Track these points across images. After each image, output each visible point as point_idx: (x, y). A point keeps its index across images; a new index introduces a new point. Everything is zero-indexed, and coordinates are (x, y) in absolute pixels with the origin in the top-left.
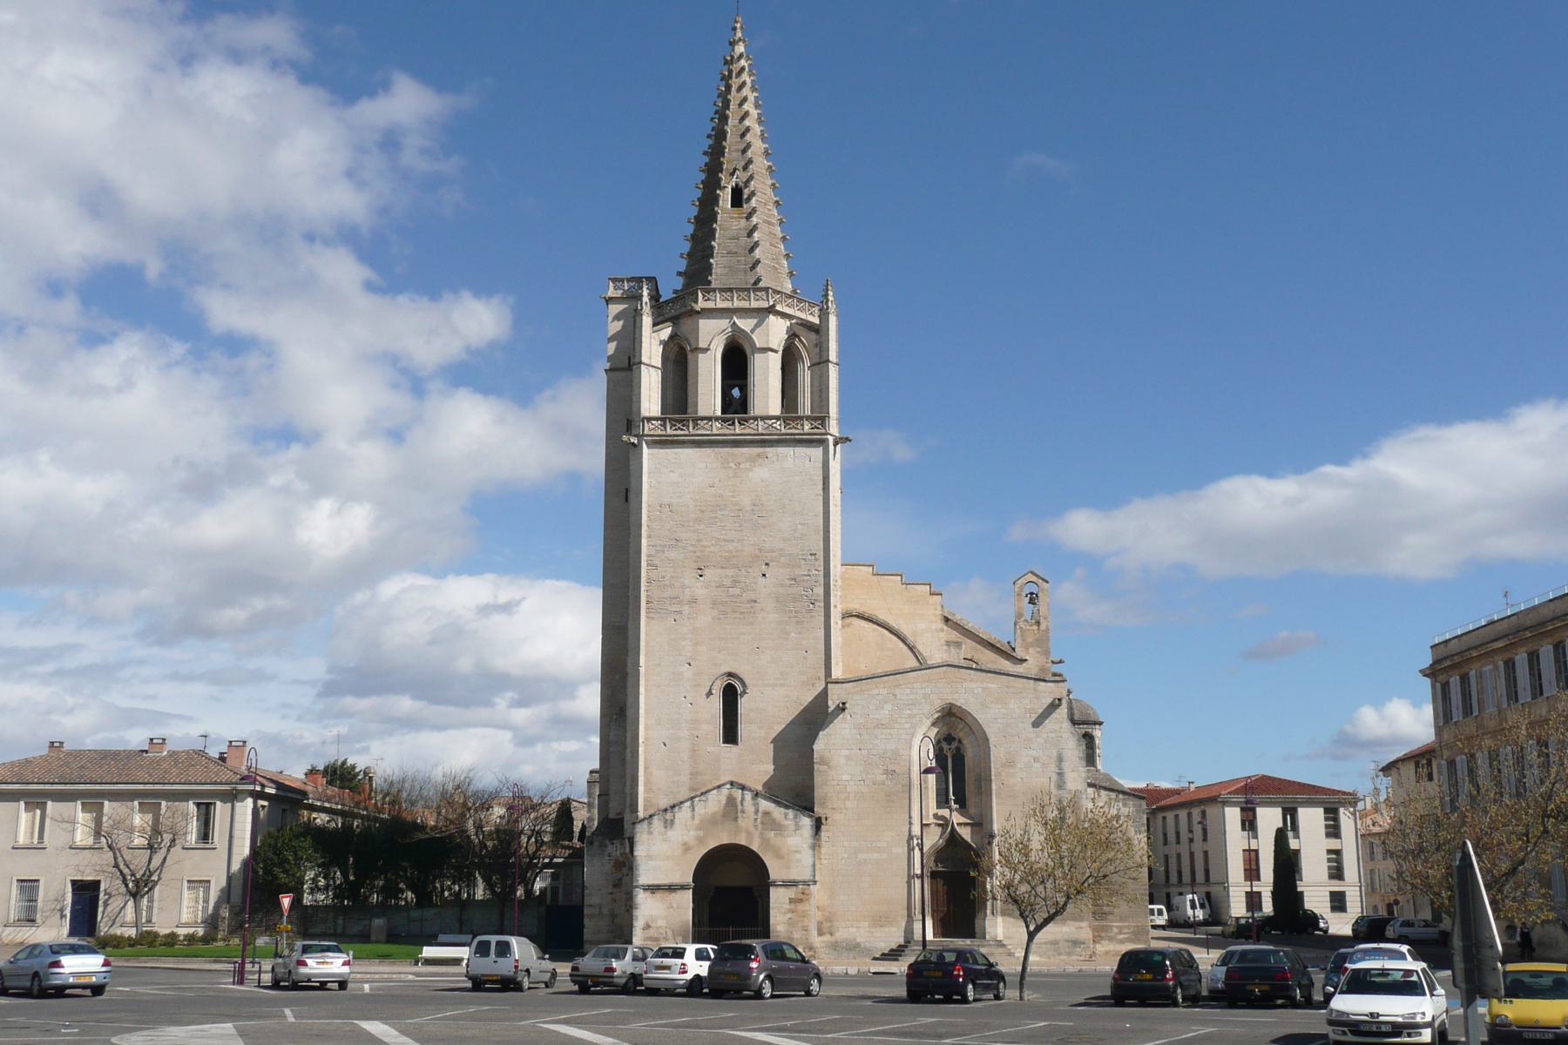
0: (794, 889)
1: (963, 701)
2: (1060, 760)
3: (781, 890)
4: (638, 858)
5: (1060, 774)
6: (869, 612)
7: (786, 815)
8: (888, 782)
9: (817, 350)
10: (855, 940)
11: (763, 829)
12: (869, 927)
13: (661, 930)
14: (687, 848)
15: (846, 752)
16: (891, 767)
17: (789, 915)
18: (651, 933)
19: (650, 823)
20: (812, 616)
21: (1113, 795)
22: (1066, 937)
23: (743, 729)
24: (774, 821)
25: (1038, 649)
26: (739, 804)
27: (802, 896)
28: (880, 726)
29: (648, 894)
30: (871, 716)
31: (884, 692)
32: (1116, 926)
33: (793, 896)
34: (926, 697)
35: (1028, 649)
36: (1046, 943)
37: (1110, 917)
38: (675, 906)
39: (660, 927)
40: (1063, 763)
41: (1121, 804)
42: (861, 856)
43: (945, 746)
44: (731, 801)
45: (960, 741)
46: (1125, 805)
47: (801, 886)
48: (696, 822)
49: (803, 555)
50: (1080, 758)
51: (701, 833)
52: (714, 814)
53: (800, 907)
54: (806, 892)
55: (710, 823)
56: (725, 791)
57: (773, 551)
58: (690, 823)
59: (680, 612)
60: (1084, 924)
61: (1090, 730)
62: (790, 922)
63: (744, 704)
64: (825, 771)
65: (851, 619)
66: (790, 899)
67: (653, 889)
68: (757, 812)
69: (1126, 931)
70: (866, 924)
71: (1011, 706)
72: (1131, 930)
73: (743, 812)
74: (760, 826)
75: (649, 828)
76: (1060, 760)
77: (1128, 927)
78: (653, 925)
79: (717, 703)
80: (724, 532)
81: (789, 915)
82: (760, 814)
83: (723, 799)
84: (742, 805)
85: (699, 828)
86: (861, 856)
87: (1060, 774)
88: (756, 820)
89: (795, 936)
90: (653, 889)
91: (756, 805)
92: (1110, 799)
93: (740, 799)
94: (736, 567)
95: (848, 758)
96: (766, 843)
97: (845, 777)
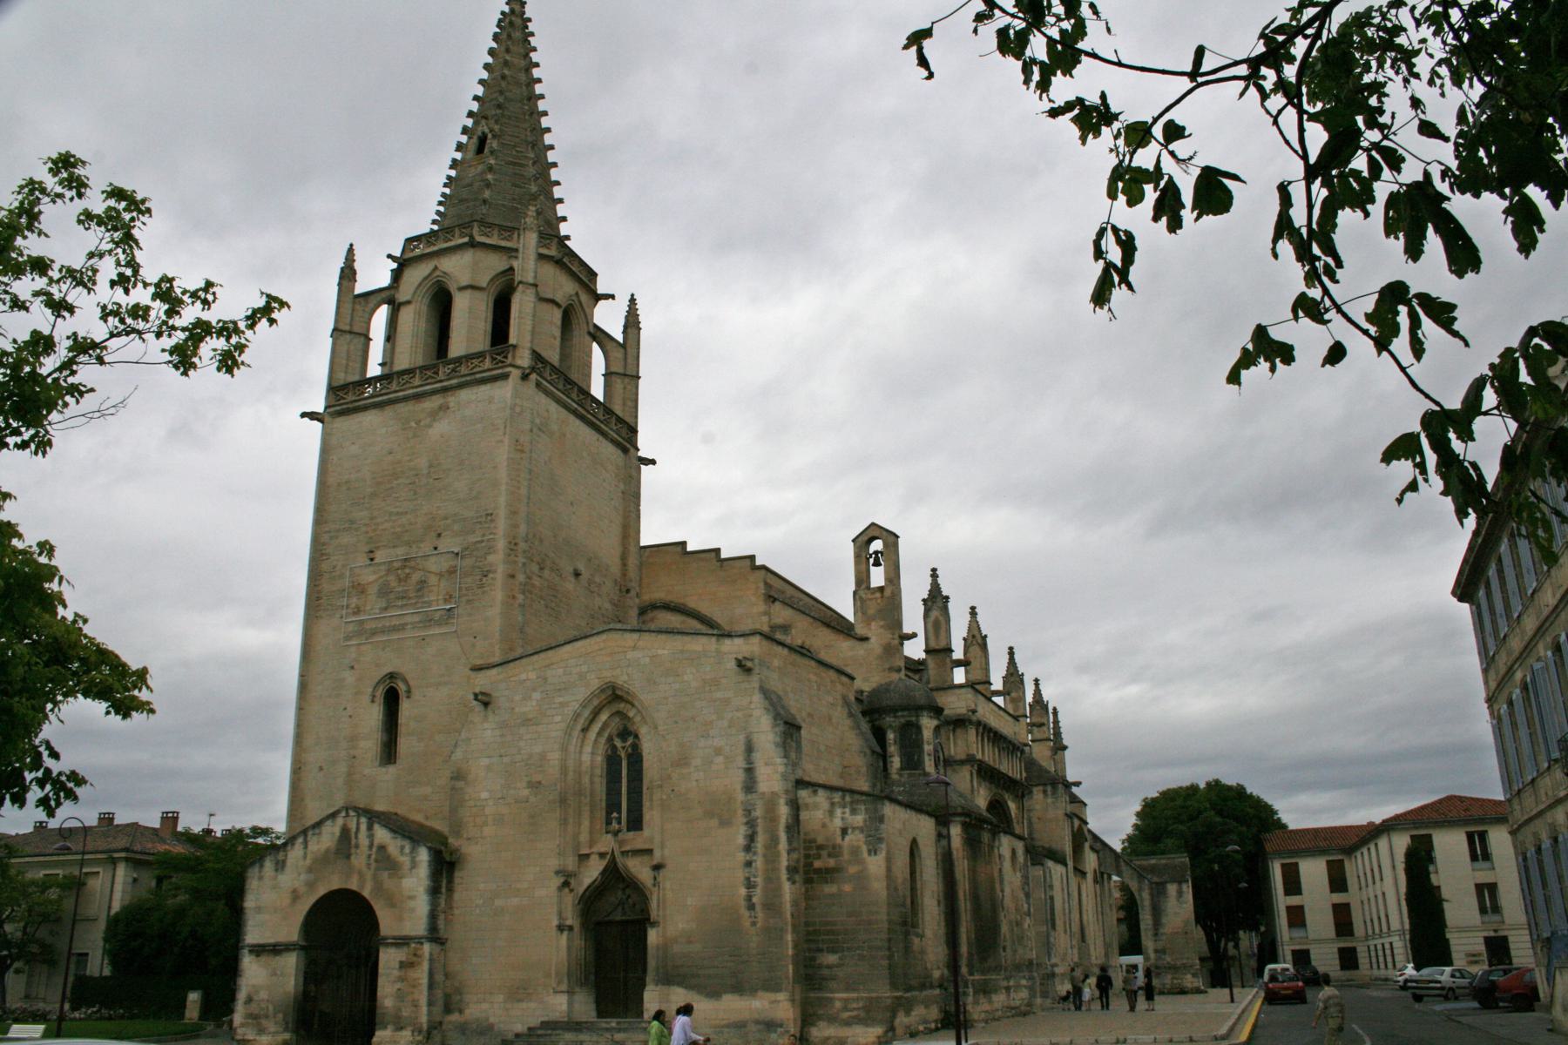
0: (405, 949)
1: (625, 678)
2: (749, 749)
3: (392, 950)
4: (247, 911)
5: (750, 771)
6: (676, 601)
7: (402, 848)
8: (532, 799)
10: (487, 1019)
11: (377, 869)
12: (505, 1002)
13: (263, 1005)
14: (296, 896)
15: (485, 761)
16: (538, 777)
17: (398, 985)
18: (254, 1007)
19: (262, 866)
20: (484, 593)
21: (837, 797)
22: (757, 1016)
23: (405, 744)
24: (388, 858)
25: (882, 623)
26: (353, 835)
27: (415, 959)
28: (527, 722)
29: (253, 957)
30: (517, 710)
31: (532, 675)
32: (840, 999)
33: (404, 959)
34: (582, 676)
35: (869, 624)
36: (728, 1026)
37: (833, 985)
38: (279, 973)
39: (263, 1000)
40: (754, 754)
41: (847, 810)
42: (498, 902)
43: (618, 743)
44: (345, 831)
45: (636, 736)
46: (854, 811)
47: (413, 945)
48: (308, 862)
49: (477, 518)
50: (777, 745)
51: (312, 877)
52: (327, 851)
54: (419, 952)
55: (321, 863)
56: (340, 821)
57: (446, 518)
58: (301, 863)
60: (782, 996)
61: (914, 719)
62: (400, 996)
63: (406, 709)
64: (461, 789)
65: (650, 615)
66: (401, 962)
67: (259, 950)
68: (371, 846)
69: (855, 1005)
70: (501, 998)
71: (686, 678)
72: (861, 1005)
73: (357, 846)
74: (374, 865)
75: (260, 872)
76: (749, 749)
77: (857, 999)
78: (255, 998)
79: (374, 715)
80: (398, 504)
81: (398, 985)
82: (374, 849)
83: (337, 830)
84: (356, 838)
85: (310, 870)
86: (498, 902)
87: (750, 771)
88: (369, 856)
89: (404, 1014)
90: (259, 950)
91: (371, 837)
92: (833, 804)
93: (354, 830)
94: (409, 544)
95: (489, 768)
96: (378, 887)
97: (484, 795)
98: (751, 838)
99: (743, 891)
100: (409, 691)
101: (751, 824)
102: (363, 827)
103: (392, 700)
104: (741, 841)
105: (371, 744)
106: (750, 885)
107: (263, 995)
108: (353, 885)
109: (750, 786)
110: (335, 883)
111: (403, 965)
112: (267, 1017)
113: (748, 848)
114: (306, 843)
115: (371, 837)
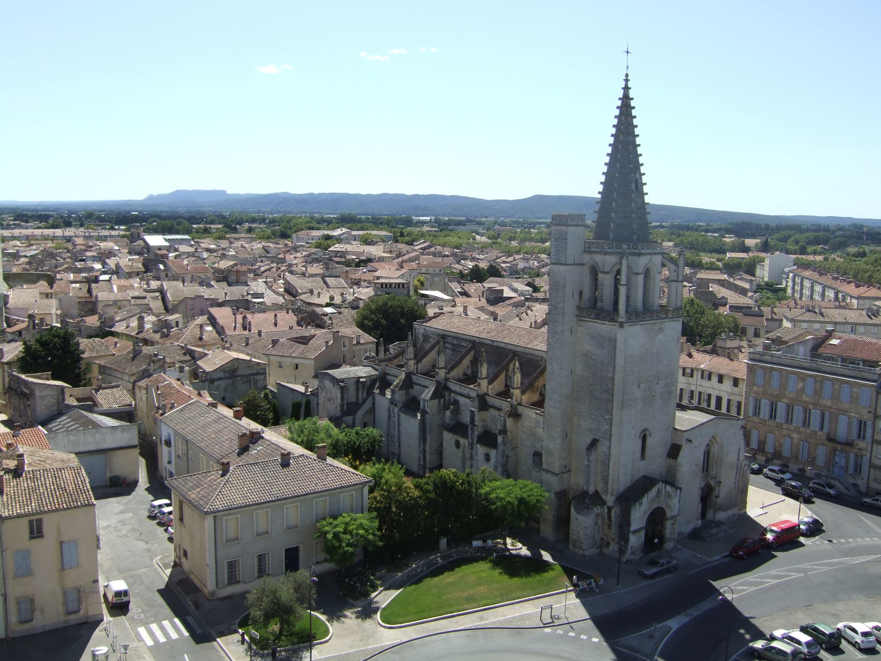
2: (739, 449)
9: (676, 274)
23: (648, 452)
44: (659, 489)
59: (631, 405)
76: (739, 449)
85: (649, 504)
90: (635, 532)
91: (665, 490)
97: (685, 470)
98: (737, 472)
99: (734, 485)
100: (650, 435)
101: (737, 469)
102: (663, 487)
103: (644, 438)
104: (735, 473)
105: (638, 454)
107: (636, 545)
108: (660, 506)
109: (738, 460)
110: (656, 506)
113: (736, 475)
115: (665, 490)
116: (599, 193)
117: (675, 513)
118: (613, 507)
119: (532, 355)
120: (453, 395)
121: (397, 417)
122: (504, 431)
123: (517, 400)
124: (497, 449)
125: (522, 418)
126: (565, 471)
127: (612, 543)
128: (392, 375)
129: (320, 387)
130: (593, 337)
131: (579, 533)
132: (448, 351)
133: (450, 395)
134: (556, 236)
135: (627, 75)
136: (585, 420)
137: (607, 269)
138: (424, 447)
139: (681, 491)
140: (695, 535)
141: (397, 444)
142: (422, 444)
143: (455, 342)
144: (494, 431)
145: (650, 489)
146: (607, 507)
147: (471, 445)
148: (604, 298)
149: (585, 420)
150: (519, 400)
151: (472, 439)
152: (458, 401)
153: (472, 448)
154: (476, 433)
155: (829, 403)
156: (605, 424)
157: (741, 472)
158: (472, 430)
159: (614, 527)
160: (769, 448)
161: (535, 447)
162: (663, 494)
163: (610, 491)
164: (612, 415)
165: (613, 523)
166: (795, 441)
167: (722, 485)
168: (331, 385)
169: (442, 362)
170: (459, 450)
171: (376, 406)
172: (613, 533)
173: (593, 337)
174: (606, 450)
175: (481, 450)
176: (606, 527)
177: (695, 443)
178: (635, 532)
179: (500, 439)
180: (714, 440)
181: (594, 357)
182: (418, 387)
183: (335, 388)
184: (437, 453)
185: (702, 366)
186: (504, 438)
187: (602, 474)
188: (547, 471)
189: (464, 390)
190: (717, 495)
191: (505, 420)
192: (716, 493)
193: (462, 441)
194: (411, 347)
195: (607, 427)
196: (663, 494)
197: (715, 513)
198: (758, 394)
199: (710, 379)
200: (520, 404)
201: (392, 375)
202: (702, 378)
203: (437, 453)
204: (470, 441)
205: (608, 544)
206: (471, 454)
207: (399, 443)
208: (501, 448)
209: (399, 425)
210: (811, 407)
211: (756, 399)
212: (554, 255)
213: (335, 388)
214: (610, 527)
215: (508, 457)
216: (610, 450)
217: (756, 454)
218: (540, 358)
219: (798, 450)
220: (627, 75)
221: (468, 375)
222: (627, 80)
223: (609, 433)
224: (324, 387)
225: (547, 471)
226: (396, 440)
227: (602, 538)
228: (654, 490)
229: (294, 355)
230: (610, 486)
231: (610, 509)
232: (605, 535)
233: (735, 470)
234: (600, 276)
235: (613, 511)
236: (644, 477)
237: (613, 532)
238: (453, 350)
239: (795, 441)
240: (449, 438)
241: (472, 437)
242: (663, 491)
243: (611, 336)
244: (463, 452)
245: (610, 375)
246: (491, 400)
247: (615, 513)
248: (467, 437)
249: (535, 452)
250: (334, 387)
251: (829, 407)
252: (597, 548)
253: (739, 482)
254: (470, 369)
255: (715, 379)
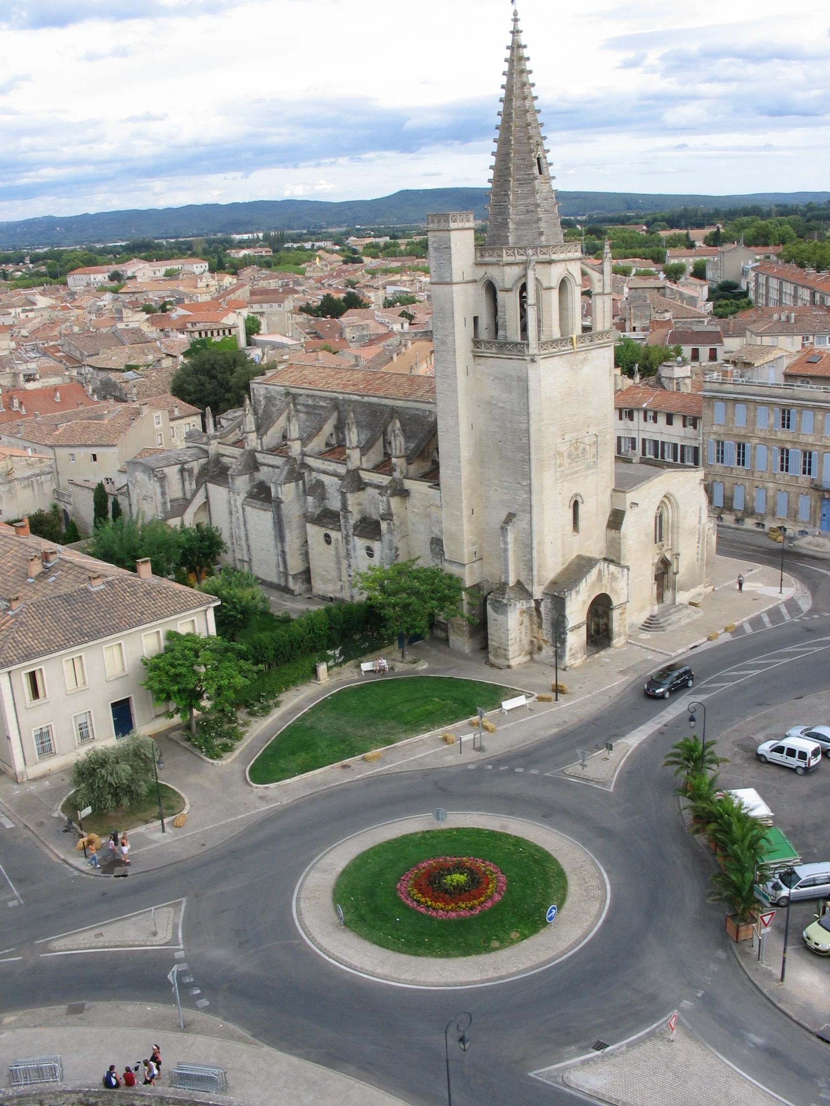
2: (700, 510)
9: (601, 284)
14: (584, 603)
18: (573, 652)
19: (571, 594)
23: (582, 524)
44: (600, 570)
53: (623, 616)
55: (593, 585)
62: (620, 625)
63: (581, 508)
90: (572, 630)
91: (608, 570)
96: (612, 589)
97: (632, 542)
98: (699, 539)
100: (582, 503)
101: (699, 534)
102: (606, 567)
103: (576, 504)
104: (697, 540)
106: (698, 554)
107: (576, 645)
108: (604, 592)
109: (700, 523)
111: (621, 614)
112: (577, 653)
113: (698, 542)
114: (586, 581)
116: (490, 181)
117: (623, 599)
118: (542, 600)
119: (417, 409)
120: (314, 474)
121: (241, 510)
122: (388, 516)
123: (402, 472)
124: (380, 540)
125: (412, 494)
126: (475, 559)
127: (544, 646)
128: (228, 456)
129: (131, 481)
130: (496, 378)
131: (500, 638)
132: (301, 415)
133: (310, 475)
134: (435, 245)
135: (515, 13)
136: (496, 490)
137: (508, 285)
138: (283, 547)
139: (628, 570)
140: (651, 624)
141: (245, 548)
142: (279, 544)
143: (310, 402)
144: (375, 517)
145: (588, 571)
146: (535, 600)
147: (346, 538)
148: (507, 324)
149: (496, 490)
150: (405, 471)
151: (346, 530)
152: (323, 482)
153: (347, 543)
154: (352, 522)
155: (811, 440)
156: (523, 492)
157: (704, 538)
158: (345, 517)
159: (546, 625)
160: (738, 504)
161: (432, 532)
162: (606, 576)
163: (536, 579)
164: (530, 479)
165: (544, 621)
166: (771, 493)
167: (680, 558)
168: (146, 478)
169: (294, 430)
170: (330, 547)
171: (211, 500)
172: (546, 633)
173: (496, 378)
174: (527, 527)
175: (360, 544)
176: (535, 627)
177: (643, 506)
178: (572, 630)
179: (384, 526)
180: (666, 500)
181: (501, 405)
182: (266, 468)
183: (152, 481)
184: (301, 554)
185: (644, 406)
186: (389, 524)
187: (525, 558)
188: (452, 562)
189: (330, 465)
190: (675, 571)
191: (388, 501)
192: (674, 568)
193: (334, 535)
194: (249, 415)
195: (525, 496)
196: (606, 576)
197: (674, 595)
198: (719, 435)
199: (655, 420)
200: (406, 477)
201: (228, 456)
202: (645, 420)
203: (301, 554)
204: (344, 532)
205: (540, 649)
206: (348, 550)
207: (248, 546)
208: (386, 538)
209: (245, 521)
210: (788, 446)
211: (718, 442)
212: (435, 271)
213: (152, 481)
214: (540, 626)
215: (397, 549)
216: (531, 526)
217: (721, 513)
218: (427, 413)
219: (775, 504)
220: (515, 13)
221: (332, 445)
222: (516, 20)
223: (529, 503)
224: (137, 481)
225: (452, 562)
226: (243, 542)
227: (532, 642)
228: (594, 572)
229: (89, 442)
230: (535, 572)
231: (537, 602)
232: (535, 638)
233: (697, 537)
234: (500, 295)
235: (542, 604)
236: (579, 557)
237: (544, 632)
238: (307, 413)
239: (771, 493)
240: (315, 533)
241: (345, 526)
242: (606, 572)
243: (520, 374)
244: (336, 548)
245: (523, 427)
246: (366, 476)
247: (546, 607)
248: (339, 530)
249: (433, 538)
250: (150, 480)
251: (812, 445)
252: (526, 655)
253: (702, 551)
254: (334, 436)
255: (662, 419)
